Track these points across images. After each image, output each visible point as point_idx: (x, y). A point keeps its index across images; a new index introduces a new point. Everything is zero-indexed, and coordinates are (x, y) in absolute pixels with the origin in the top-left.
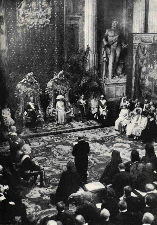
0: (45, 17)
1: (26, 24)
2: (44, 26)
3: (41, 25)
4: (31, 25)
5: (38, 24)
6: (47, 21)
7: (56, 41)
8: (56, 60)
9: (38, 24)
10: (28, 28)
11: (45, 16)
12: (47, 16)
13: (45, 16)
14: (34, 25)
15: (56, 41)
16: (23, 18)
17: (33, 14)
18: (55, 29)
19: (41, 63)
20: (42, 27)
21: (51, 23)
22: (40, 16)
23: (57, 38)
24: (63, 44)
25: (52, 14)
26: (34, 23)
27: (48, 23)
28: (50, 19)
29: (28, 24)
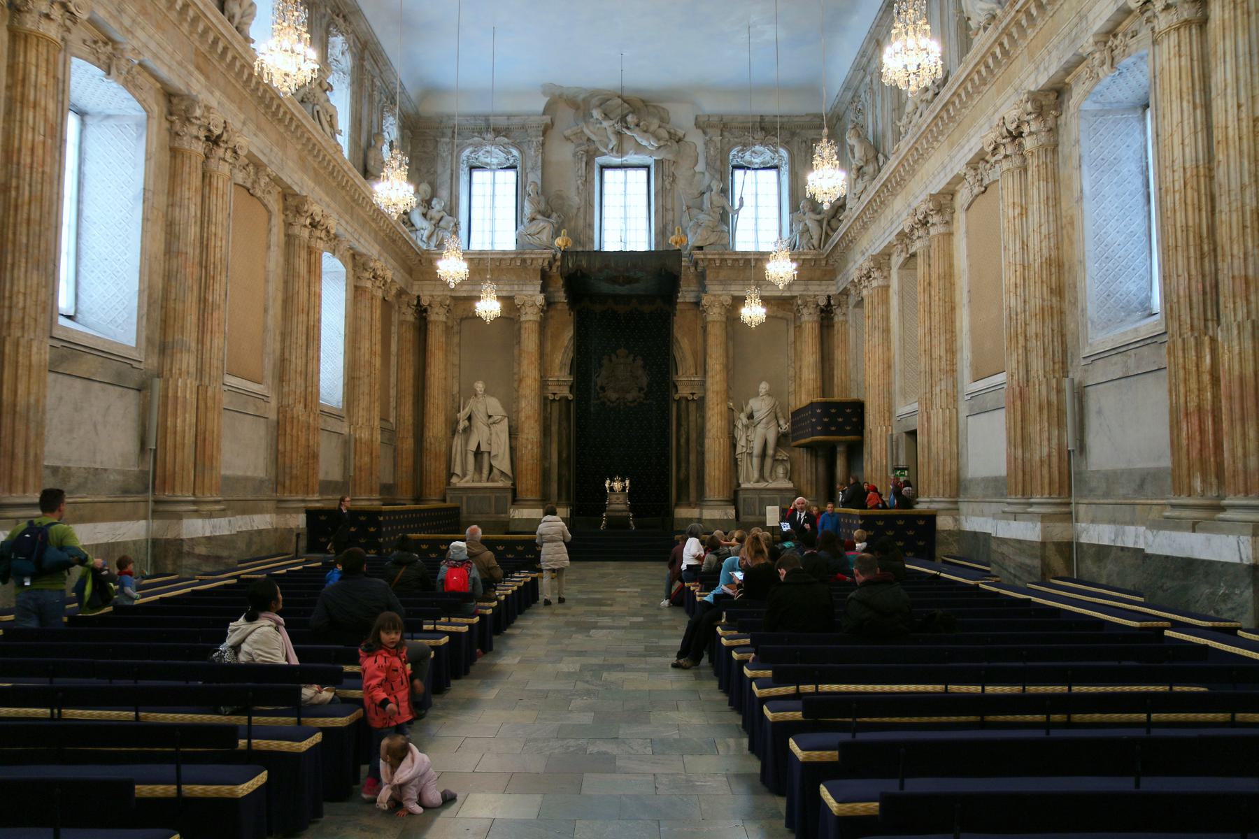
12: (641, 389)
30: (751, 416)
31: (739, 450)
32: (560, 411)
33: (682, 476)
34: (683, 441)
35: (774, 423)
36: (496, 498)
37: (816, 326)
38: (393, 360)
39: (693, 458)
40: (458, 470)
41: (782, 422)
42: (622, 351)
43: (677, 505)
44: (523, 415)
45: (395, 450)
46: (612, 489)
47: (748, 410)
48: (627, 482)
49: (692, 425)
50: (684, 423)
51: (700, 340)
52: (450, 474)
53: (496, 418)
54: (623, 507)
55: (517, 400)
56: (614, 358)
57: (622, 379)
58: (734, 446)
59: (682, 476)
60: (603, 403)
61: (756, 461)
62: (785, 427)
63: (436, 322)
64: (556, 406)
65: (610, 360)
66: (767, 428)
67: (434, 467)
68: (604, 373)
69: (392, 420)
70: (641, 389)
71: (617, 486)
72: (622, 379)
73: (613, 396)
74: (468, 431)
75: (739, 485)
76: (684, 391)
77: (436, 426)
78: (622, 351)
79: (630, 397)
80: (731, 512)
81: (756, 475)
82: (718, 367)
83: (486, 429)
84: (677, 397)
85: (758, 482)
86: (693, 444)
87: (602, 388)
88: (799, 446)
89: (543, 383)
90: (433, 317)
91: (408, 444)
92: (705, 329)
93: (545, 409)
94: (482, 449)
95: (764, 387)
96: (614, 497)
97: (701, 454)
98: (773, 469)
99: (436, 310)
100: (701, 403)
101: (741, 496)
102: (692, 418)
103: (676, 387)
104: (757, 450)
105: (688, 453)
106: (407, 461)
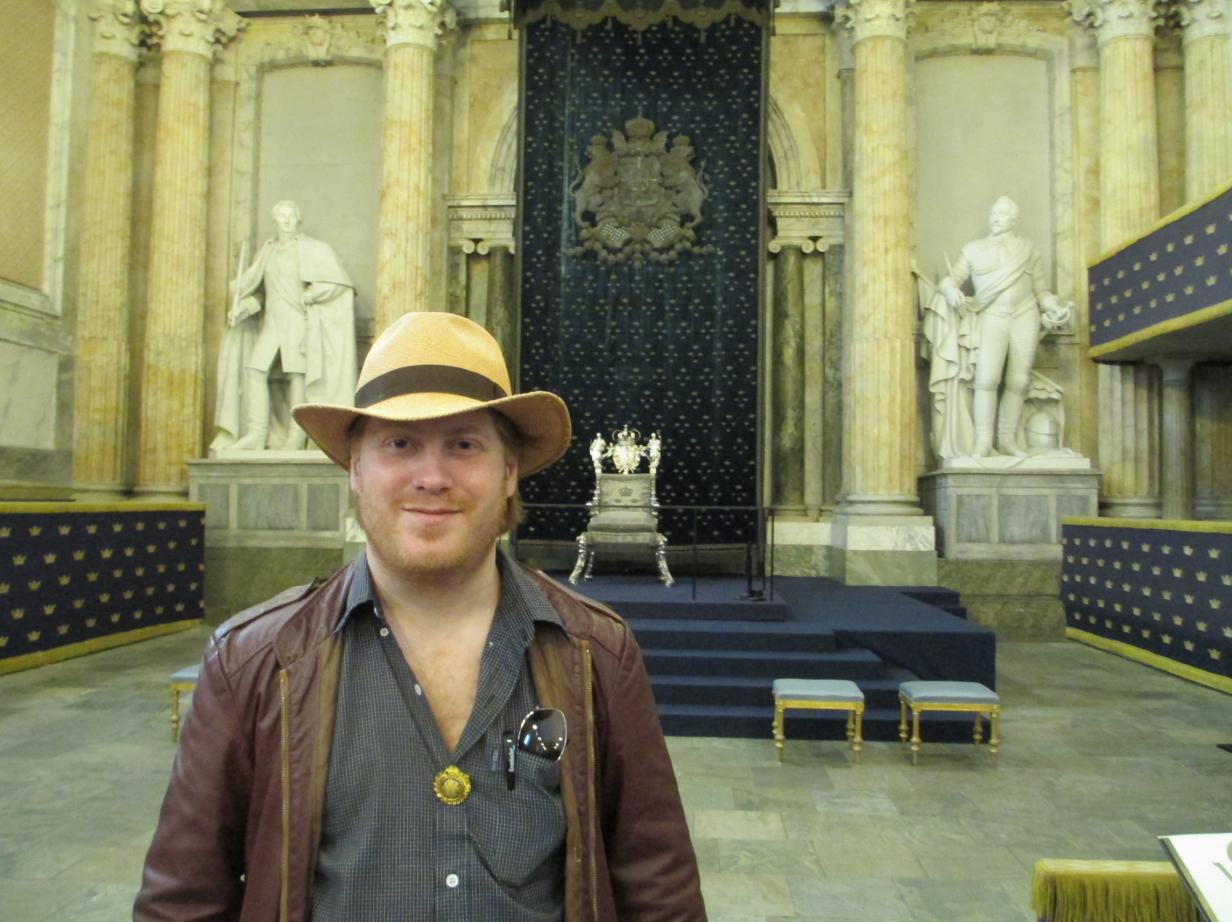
1: (598, 246)
2: (672, 254)
3: (655, 250)
6: (683, 238)
8: (718, 392)
12: (686, 218)
14: (627, 249)
16: (586, 224)
19: (647, 402)
20: (664, 257)
21: (698, 242)
24: (750, 326)
25: (707, 208)
26: (628, 242)
27: (688, 244)
28: (696, 229)
29: (605, 247)
30: (968, 288)
31: (938, 371)
32: (491, 283)
33: (787, 442)
34: (789, 354)
35: (1030, 303)
36: (313, 491)
37: (1144, 49)
38: (58, 142)
39: (812, 397)
40: (226, 418)
41: (1049, 301)
42: (639, 124)
43: (772, 512)
44: (384, 282)
45: (66, 365)
46: (609, 466)
47: (960, 272)
48: (655, 445)
49: (813, 317)
50: (792, 310)
51: (832, 104)
52: (209, 431)
53: (317, 289)
54: (641, 517)
55: (371, 246)
56: (618, 140)
57: (641, 194)
58: (924, 366)
59: (787, 442)
60: (591, 255)
61: (984, 399)
62: (1067, 306)
63: (178, 53)
64: (480, 271)
65: (610, 147)
66: (1013, 316)
67: (168, 412)
68: (592, 177)
69: (52, 283)
70: (686, 218)
71: (626, 454)
72: (641, 194)
73: (616, 236)
74: (256, 321)
75: (933, 460)
76: (792, 232)
77: (174, 308)
78: (639, 124)
79: (657, 238)
80: (923, 534)
81: (985, 438)
82: (888, 156)
83: (296, 316)
84: (774, 246)
85: (988, 455)
86: (813, 366)
87: (589, 216)
88: (1108, 360)
89: (446, 212)
90: (172, 42)
91: (104, 357)
92: (847, 78)
93: (453, 277)
94: (287, 367)
95: (1004, 210)
96: (608, 489)
97: (835, 387)
98: (1024, 425)
99: (178, 25)
100: (833, 260)
101: (950, 492)
102: (812, 298)
103: (772, 222)
104: (988, 374)
105: (802, 384)
106: (99, 401)
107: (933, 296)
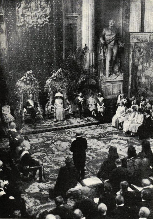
0: (44, 17)
1: (26, 23)
2: (43, 25)
3: (40, 24)
4: (30, 24)
5: (37, 23)
6: (45, 21)
7: (54, 40)
8: (55, 59)
9: (37, 23)
10: (28, 27)
11: (44, 16)
12: (46, 16)
13: (44, 16)
14: (33, 24)
15: (54, 40)
16: (23, 18)
17: (32, 13)
18: (54, 28)
19: (40, 62)
20: (41, 26)
21: (49, 22)
22: (39, 15)
23: (55, 37)
24: (61, 43)
25: (51, 13)
26: (33, 22)
27: (47, 23)
28: (49, 19)
29: (27, 23)
107: (101, 57)
